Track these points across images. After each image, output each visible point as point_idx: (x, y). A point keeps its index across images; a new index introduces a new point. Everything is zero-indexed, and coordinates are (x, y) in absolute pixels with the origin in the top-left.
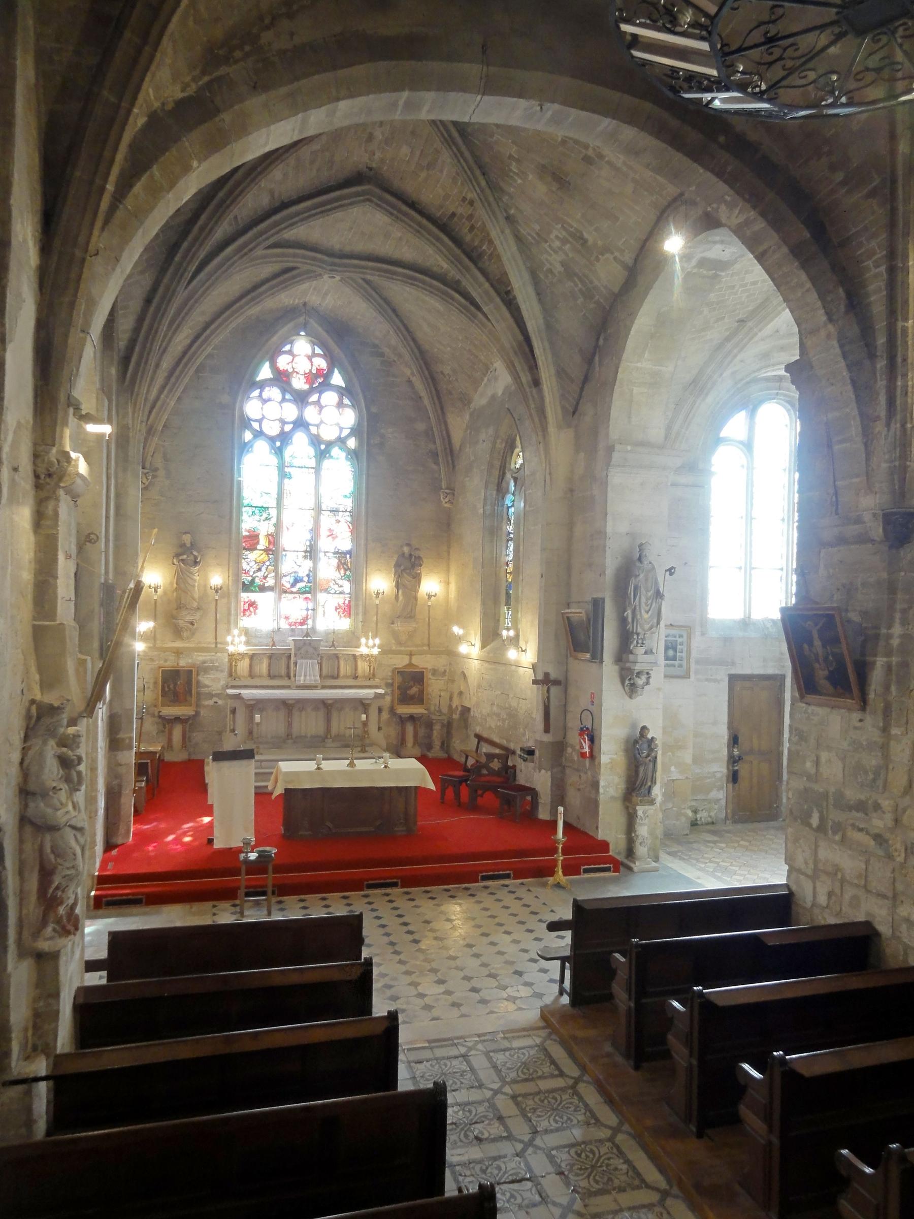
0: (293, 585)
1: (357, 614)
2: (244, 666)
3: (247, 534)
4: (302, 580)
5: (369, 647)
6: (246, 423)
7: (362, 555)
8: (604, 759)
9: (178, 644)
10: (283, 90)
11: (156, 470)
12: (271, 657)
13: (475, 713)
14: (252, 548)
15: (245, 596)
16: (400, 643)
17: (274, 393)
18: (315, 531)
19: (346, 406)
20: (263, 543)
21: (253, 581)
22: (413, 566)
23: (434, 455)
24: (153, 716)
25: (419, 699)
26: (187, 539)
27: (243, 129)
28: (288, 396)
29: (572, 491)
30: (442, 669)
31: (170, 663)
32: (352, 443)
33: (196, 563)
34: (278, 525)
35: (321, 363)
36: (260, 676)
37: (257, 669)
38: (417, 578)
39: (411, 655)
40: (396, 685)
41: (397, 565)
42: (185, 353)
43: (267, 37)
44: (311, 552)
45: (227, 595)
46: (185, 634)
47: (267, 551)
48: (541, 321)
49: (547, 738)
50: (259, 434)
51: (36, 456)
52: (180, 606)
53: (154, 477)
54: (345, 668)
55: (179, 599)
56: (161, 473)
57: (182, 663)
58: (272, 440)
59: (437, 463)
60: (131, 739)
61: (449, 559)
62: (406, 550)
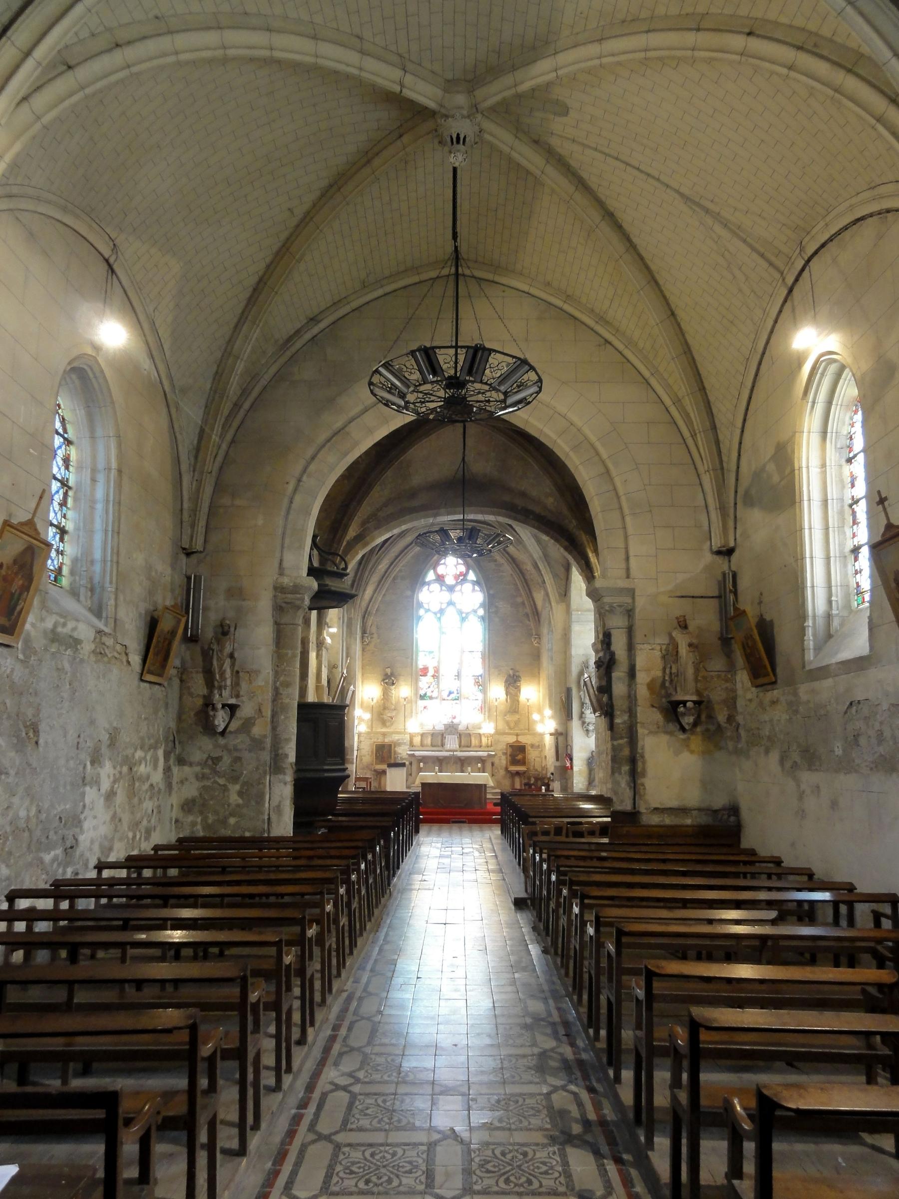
0: (448, 696)
1: (485, 711)
2: (417, 740)
3: (422, 667)
4: (453, 693)
5: (488, 728)
6: (420, 605)
7: (487, 676)
8: (575, 769)
9: (384, 730)
10: (384, 527)
11: (373, 634)
12: (433, 735)
13: (548, 767)
14: (425, 675)
15: (421, 703)
16: (510, 728)
17: (435, 587)
18: (461, 663)
19: (477, 591)
20: (431, 672)
21: (425, 694)
22: (515, 682)
23: (527, 615)
24: (371, 770)
25: (523, 762)
26: (389, 671)
27: (373, 539)
28: (444, 588)
29: (566, 634)
30: (537, 744)
31: (380, 740)
32: (481, 612)
33: (393, 684)
34: (439, 662)
35: (462, 569)
36: (427, 746)
37: (425, 742)
38: (518, 689)
39: (517, 735)
40: (509, 753)
41: (506, 681)
42: (386, 572)
43: (379, 514)
44: (458, 676)
45: (410, 702)
46: (388, 724)
47: (433, 676)
48: (541, 553)
49: (558, 764)
50: (427, 610)
51: (317, 639)
52: (385, 708)
53: (372, 638)
54: (474, 742)
55: (384, 703)
56: (375, 636)
57: (386, 740)
58: (435, 614)
59: (529, 620)
60: (353, 759)
61: (539, 677)
62: (511, 672)
